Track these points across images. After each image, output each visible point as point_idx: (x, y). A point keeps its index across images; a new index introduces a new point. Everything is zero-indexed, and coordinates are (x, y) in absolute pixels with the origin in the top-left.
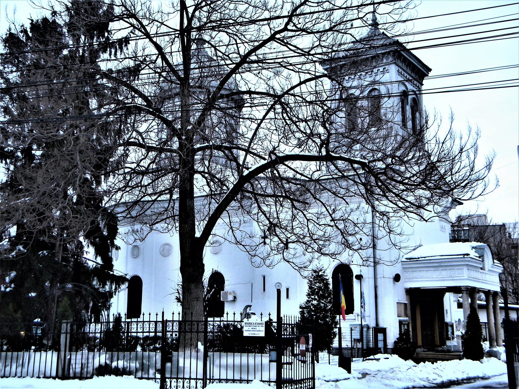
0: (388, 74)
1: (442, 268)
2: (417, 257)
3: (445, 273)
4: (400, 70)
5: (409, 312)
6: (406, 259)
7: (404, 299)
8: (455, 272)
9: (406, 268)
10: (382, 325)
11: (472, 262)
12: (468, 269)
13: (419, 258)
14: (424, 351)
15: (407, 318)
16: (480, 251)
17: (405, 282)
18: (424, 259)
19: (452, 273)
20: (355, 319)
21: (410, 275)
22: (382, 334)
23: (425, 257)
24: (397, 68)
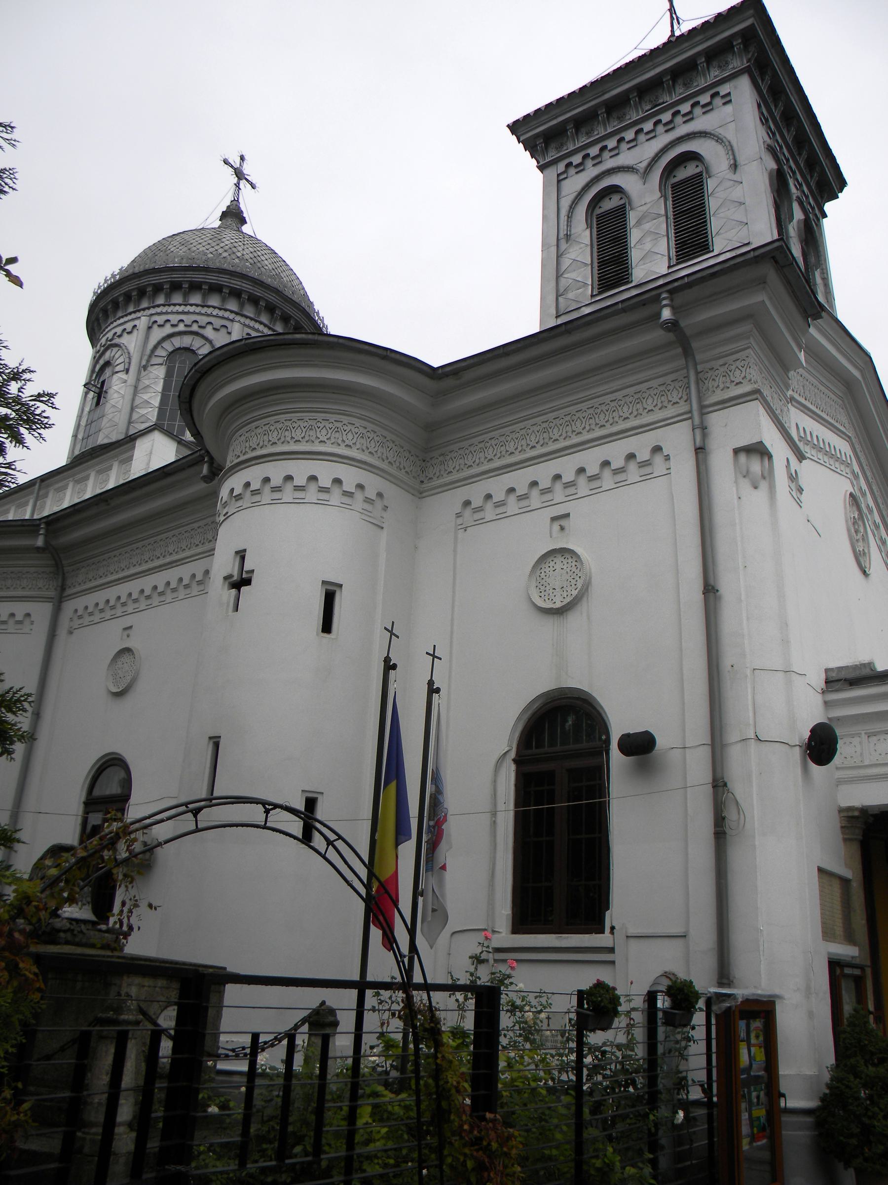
0: (729, 108)
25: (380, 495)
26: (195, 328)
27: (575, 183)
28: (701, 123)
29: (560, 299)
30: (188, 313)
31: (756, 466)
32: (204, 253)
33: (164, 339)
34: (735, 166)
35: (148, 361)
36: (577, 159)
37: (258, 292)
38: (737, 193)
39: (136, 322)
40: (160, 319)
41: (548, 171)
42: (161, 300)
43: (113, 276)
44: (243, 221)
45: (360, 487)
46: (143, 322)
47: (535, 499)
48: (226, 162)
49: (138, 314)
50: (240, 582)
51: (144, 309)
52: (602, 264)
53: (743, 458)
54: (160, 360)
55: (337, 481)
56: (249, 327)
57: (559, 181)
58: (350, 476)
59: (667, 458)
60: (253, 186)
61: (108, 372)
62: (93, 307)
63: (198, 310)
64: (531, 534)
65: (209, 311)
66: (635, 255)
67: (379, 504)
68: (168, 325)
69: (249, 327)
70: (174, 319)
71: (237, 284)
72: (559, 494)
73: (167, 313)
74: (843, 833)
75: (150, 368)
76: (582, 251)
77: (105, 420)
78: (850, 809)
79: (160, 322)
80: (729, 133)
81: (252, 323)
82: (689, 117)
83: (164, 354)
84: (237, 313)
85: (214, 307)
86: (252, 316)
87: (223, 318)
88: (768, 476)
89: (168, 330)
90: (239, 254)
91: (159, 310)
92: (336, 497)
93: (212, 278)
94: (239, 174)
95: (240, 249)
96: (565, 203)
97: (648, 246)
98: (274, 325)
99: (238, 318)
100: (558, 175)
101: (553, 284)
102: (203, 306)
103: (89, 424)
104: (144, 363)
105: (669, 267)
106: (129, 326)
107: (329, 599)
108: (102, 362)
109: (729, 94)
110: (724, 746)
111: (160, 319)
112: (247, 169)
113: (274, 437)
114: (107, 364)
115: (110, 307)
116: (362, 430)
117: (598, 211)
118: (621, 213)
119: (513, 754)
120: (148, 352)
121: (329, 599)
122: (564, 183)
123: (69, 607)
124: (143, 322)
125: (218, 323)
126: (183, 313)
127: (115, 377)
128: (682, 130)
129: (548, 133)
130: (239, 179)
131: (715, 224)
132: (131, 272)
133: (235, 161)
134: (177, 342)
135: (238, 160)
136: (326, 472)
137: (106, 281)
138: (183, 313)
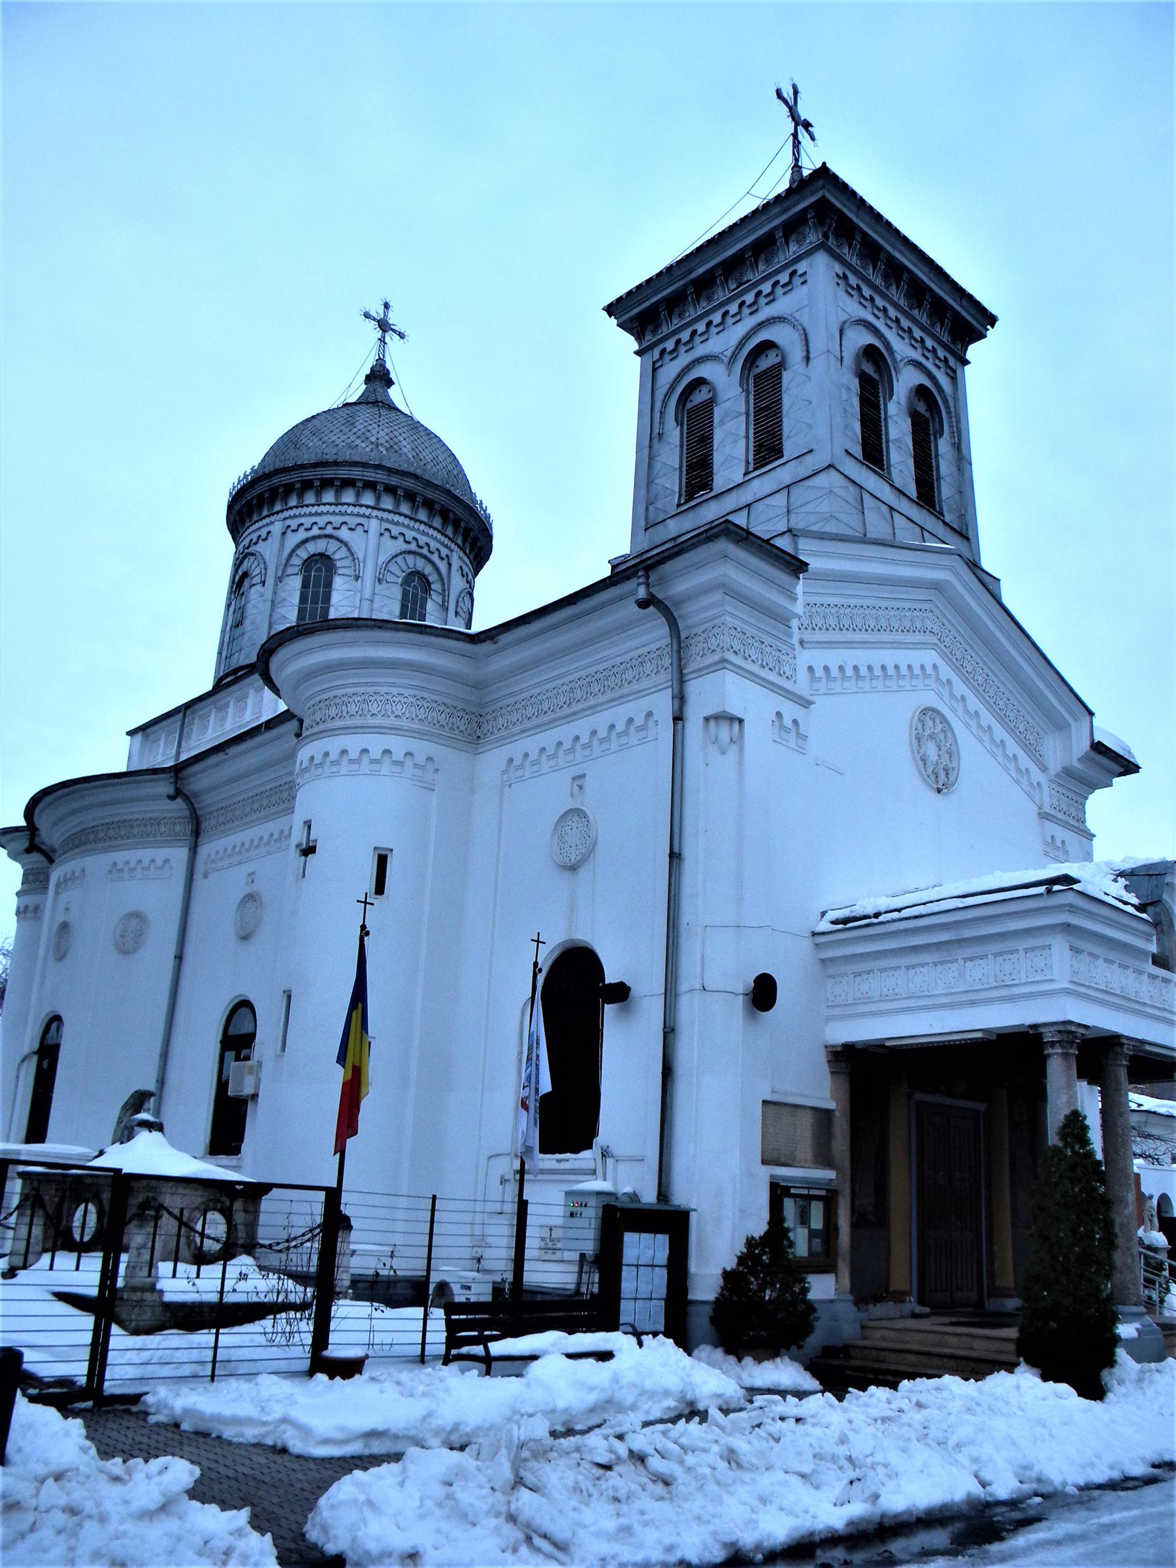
0: (805, 287)
1: (967, 952)
2: (870, 911)
3: (979, 972)
4: (853, 280)
5: (841, 1145)
6: (832, 923)
7: (820, 1089)
8: (1020, 966)
9: (831, 960)
10: (681, 1197)
11: (1091, 915)
12: (1075, 950)
13: (877, 915)
14: (914, 1316)
15: (831, 1174)
16: (1146, 885)
17: (829, 1019)
18: (896, 915)
19: (1007, 967)
20: (594, 1172)
21: (844, 989)
22: (663, 1240)
23: (899, 910)
24: (838, 268)
25: (429, 759)
28: (783, 305)
29: (651, 508)
30: (322, 514)
31: (724, 732)
33: (298, 546)
35: (284, 571)
36: (670, 345)
37: (394, 481)
39: (270, 528)
40: (293, 524)
41: (648, 356)
42: (293, 502)
43: (246, 476)
44: (390, 383)
45: (409, 754)
46: (277, 528)
47: (562, 760)
48: (367, 315)
49: (272, 518)
50: (309, 850)
51: (277, 513)
52: (691, 468)
53: (712, 723)
54: (296, 570)
55: (387, 752)
56: (387, 521)
57: (654, 370)
58: (398, 745)
60: (402, 336)
61: (246, 583)
62: (230, 507)
63: (332, 509)
64: (548, 794)
65: (344, 509)
66: (717, 458)
67: (430, 767)
68: (302, 529)
69: (387, 521)
70: (307, 521)
71: (370, 475)
72: (579, 754)
73: (300, 516)
74: (830, 1066)
75: (286, 580)
76: (671, 455)
77: (246, 638)
78: (833, 1046)
79: (294, 527)
80: (804, 319)
81: (391, 516)
82: (771, 297)
83: (299, 562)
84: (373, 508)
85: (349, 505)
86: (390, 508)
87: (358, 515)
88: (738, 741)
89: (302, 535)
90: (373, 439)
91: (291, 512)
92: (387, 767)
93: (343, 473)
94: (384, 326)
95: (374, 432)
96: (660, 395)
97: (728, 449)
98: (417, 511)
99: (375, 513)
100: (654, 363)
101: (643, 492)
102: (336, 505)
103: (232, 640)
104: (279, 574)
106: (263, 533)
107: (382, 861)
108: (240, 572)
109: (805, 273)
110: (676, 995)
111: (293, 524)
112: (393, 319)
114: (246, 575)
115: (248, 506)
116: (411, 699)
117: (689, 406)
118: (709, 406)
120: (284, 562)
121: (382, 861)
122: (660, 371)
123: (207, 849)
124: (277, 528)
126: (316, 514)
127: (254, 589)
128: (765, 313)
130: (384, 331)
132: (261, 472)
133: (377, 310)
134: (312, 548)
135: (381, 309)
136: (376, 743)
137: (239, 481)
138: (316, 514)
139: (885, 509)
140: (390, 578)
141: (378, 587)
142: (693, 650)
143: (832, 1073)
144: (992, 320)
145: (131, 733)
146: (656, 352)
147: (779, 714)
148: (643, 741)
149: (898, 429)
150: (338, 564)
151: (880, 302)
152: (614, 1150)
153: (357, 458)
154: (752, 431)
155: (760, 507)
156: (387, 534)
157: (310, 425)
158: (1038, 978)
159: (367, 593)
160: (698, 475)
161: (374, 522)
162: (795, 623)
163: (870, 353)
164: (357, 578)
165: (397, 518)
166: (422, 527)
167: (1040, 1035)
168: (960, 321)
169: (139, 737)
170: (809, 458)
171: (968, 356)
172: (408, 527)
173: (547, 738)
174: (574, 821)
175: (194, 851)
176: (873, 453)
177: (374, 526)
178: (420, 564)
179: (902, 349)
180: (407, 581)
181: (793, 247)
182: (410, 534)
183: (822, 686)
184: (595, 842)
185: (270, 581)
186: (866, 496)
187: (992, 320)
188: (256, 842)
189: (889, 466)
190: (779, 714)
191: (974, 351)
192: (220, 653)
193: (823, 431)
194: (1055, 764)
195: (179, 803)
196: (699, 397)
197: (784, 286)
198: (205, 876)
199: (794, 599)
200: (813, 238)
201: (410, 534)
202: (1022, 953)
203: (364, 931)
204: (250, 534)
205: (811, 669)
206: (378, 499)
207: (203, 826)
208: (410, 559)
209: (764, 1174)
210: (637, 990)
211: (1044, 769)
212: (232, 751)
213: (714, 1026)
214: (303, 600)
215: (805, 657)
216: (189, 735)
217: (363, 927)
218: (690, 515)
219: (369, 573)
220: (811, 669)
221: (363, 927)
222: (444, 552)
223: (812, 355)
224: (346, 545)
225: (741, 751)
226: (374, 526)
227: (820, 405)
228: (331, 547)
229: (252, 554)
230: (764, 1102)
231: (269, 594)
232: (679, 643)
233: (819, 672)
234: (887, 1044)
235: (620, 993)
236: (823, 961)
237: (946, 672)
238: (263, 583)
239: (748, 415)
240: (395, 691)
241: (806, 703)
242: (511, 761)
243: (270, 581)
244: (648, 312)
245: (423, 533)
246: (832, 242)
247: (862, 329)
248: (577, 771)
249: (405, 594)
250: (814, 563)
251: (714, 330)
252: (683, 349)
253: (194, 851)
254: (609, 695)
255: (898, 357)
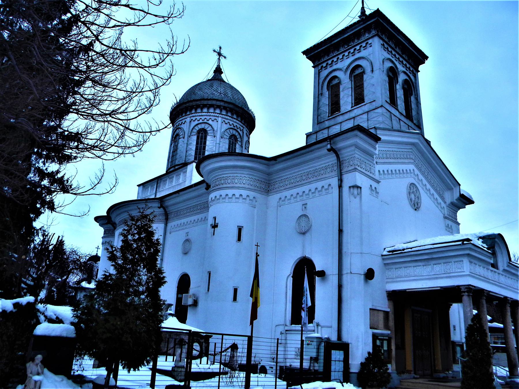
0: (371, 48)
1: (434, 262)
2: (401, 248)
3: (439, 268)
4: (386, 46)
5: (391, 323)
6: (388, 252)
7: (384, 305)
8: (453, 267)
9: (388, 264)
10: (346, 338)
11: (475, 251)
12: (471, 262)
13: (404, 250)
14: (414, 378)
15: (389, 332)
16: (489, 242)
17: (387, 282)
18: (410, 250)
19: (448, 267)
20: (314, 331)
21: (393, 273)
22: (342, 352)
23: (411, 248)
24: (382, 42)
25: (254, 198)
26: (205, 121)
27: (324, 73)
28: (364, 53)
29: (319, 117)
31: (356, 191)
32: (208, 93)
34: (372, 71)
36: (324, 65)
37: (226, 105)
38: (373, 81)
39: (186, 120)
40: (194, 118)
41: (317, 68)
42: (193, 111)
45: (248, 196)
46: (188, 120)
47: (299, 198)
48: (214, 51)
49: (186, 117)
50: (215, 226)
52: (332, 105)
54: (194, 134)
55: (241, 195)
56: (224, 118)
57: (319, 73)
58: (245, 193)
59: (332, 188)
60: (225, 58)
62: (171, 113)
63: (206, 114)
64: (295, 210)
65: (210, 114)
66: (342, 102)
67: (254, 200)
68: (196, 121)
69: (224, 118)
71: (218, 103)
72: (304, 197)
73: (196, 116)
76: (325, 100)
80: (371, 58)
81: (225, 117)
87: (215, 116)
88: (360, 194)
89: (196, 122)
91: (193, 115)
92: (241, 200)
93: (210, 102)
94: (220, 54)
97: (345, 99)
99: (220, 115)
101: (316, 112)
103: (173, 156)
105: (352, 107)
106: (183, 121)
107: (240, 230)
108: (175, 134)
110: (342, 275)
112: (222, 52)
113: (223, 182)
115: (178, 113)
119: (292, 275)
121: (240, 230)
123: (170, 225)
124: (188, 120)
125: (213, 118)
126: (201, 116)
127: (180, 140)
128: (357, 56)
129: (317, 54)
130: (220, 56)
131: (366, 92)
133: (217, 49)
134: (200, 127)
136: (237, 192)
138: (201, 116)
139: (398, 119)
140: (225, 137)
141: (221, 140)
142: (344, 165)
143: (388, 300)
144: (427, 58)
145: (139, 186)
146: (320, 67)
147: (371, 186)
148: (327, 194)
149: (400, 93)
150: (209, 132)
151: (394, 53)
152: (322, 324)
153: (214, 98)
154: (353, 94)
155: (358, 118)
156: (224, 123)
157: (198, 87)
158: (459, 271)
159: (218, 142)
160: (335, 107)
161: (220, 118)
162: (375, 157)
163: (391, 68)
164: (215, 137)
165: (227, 117)
166: (235, 120)
167: (461, 289)
168: (416, 58)
169: (141, 187)
170: (374, 103)
171: (419, 69)
172: (230, 120)
173: (294, 191)
174: (304, 219)
175: (166, 225)
176: (393, 101)
177: (220, 120)
178: (234, 132)
179: (400, 68)
180: (230, 138)
181: (367, 35)
182: (231, 123)
183: (382, 176)
184: (311, 226)
185: (186, 137)
186: (392, 115)
187: (427, 58)
188: (189, 223)
189: (397, 105)
190: (371, 186)
191: (421, 68)
192: (168, 160)
193: (378, 94)
194: (448, 201)
195: (162, 209)
196: (336, 81)
197: (364, 47)
198: (170, 233)
199: (376, 149)
200: (374, 32)
201: (231, 123)
202: (453, 263)
203: (257, 255)
204: (178, 122)
205: (379, 171)
206: (221, 111)
207: (169, 217)
208: (231, 130)
209: (371, 331)
210: (327, 272)
211: (445, 203)
212: (181, 193)
213: (354, 284)
214: (197, 143)
215: (378, 167)
216: (160, 186)
217: (257, 253)
218: (333, 120)
219: (218, 136)
220: (379, 171)
221: (257, 253)
222: (242, 128)
223: (374, 70)
224: (211, 126)
225: (361, 197)
226: (220, 120)
227: (376, 85)
228: (206, 126)
229: (179, 128)
230: (370, 309)
231: (186, 142)
232: (340, 162)
233: (382, 172)
234: (407, 291)
235: (322, 274)
236: (385, 264)
237: (417, 172)
238: (184, 138)
239: (352, 88)
240: (243, 175)
241: (378, 182)
242: (280, 198)
243: (186, 137)
244: (317, 54)
245: (235, 122)
246: (380, 34)
247: (389, 61)
248: (304, 202)
249: (230, 142)
250: (383, 138)
251: (339, 61)
252: (329, 66)
253: (166, 225)
254: (315, 179)
255: (399, 70)
